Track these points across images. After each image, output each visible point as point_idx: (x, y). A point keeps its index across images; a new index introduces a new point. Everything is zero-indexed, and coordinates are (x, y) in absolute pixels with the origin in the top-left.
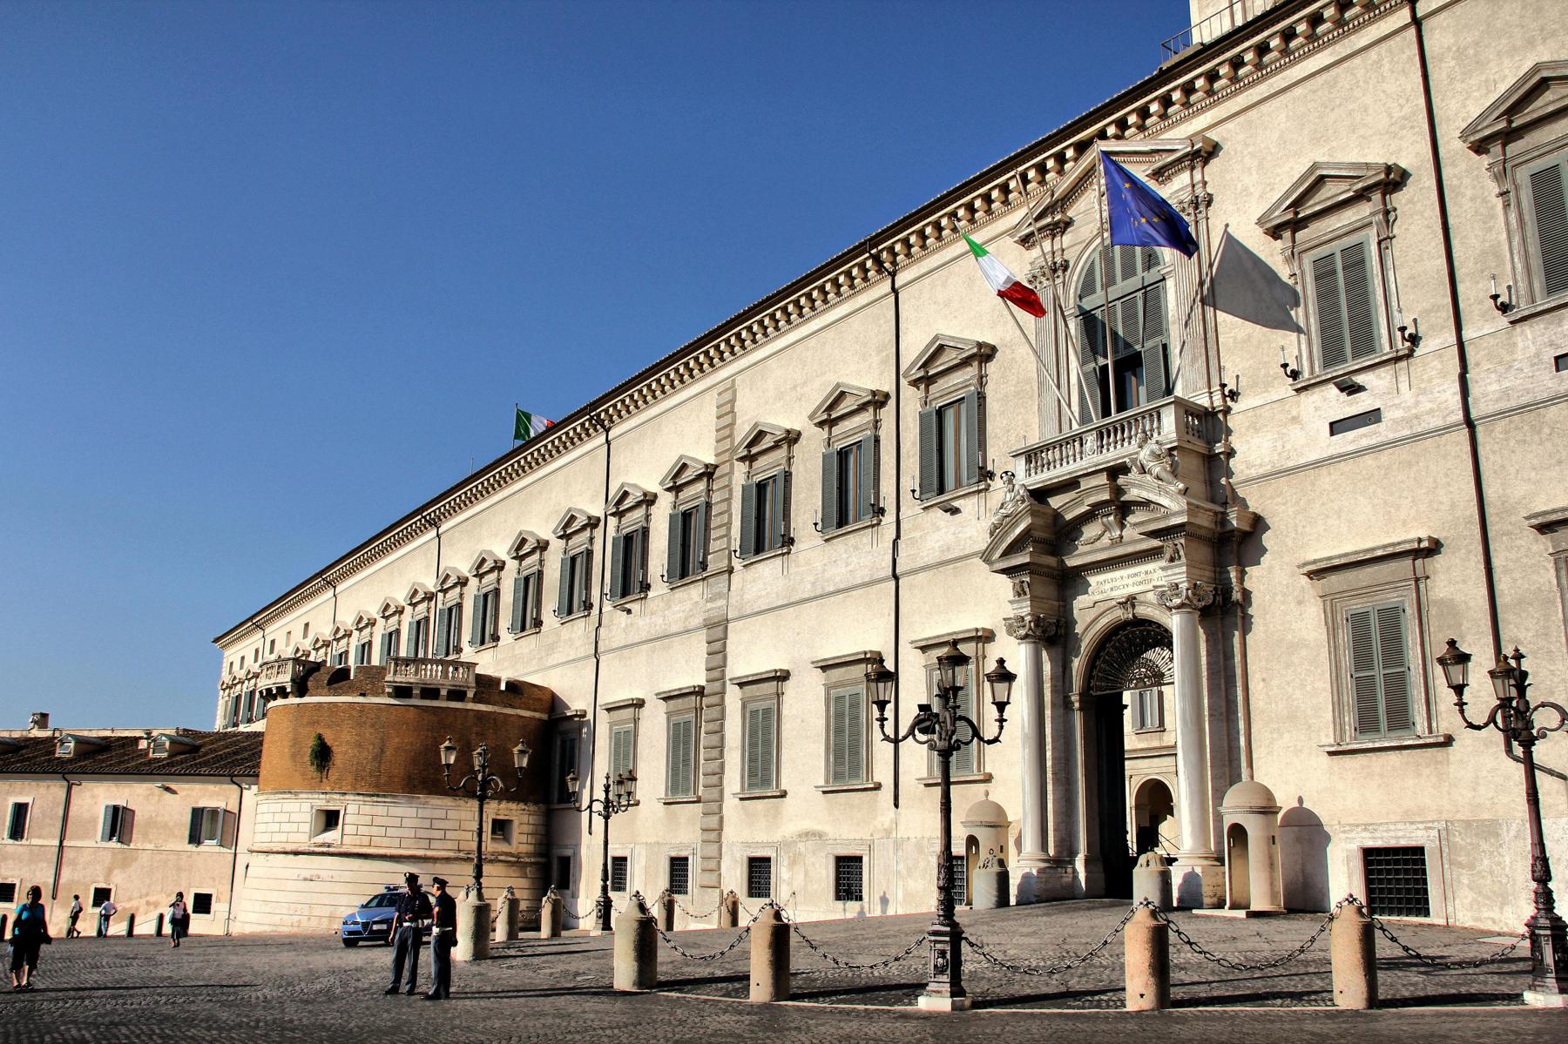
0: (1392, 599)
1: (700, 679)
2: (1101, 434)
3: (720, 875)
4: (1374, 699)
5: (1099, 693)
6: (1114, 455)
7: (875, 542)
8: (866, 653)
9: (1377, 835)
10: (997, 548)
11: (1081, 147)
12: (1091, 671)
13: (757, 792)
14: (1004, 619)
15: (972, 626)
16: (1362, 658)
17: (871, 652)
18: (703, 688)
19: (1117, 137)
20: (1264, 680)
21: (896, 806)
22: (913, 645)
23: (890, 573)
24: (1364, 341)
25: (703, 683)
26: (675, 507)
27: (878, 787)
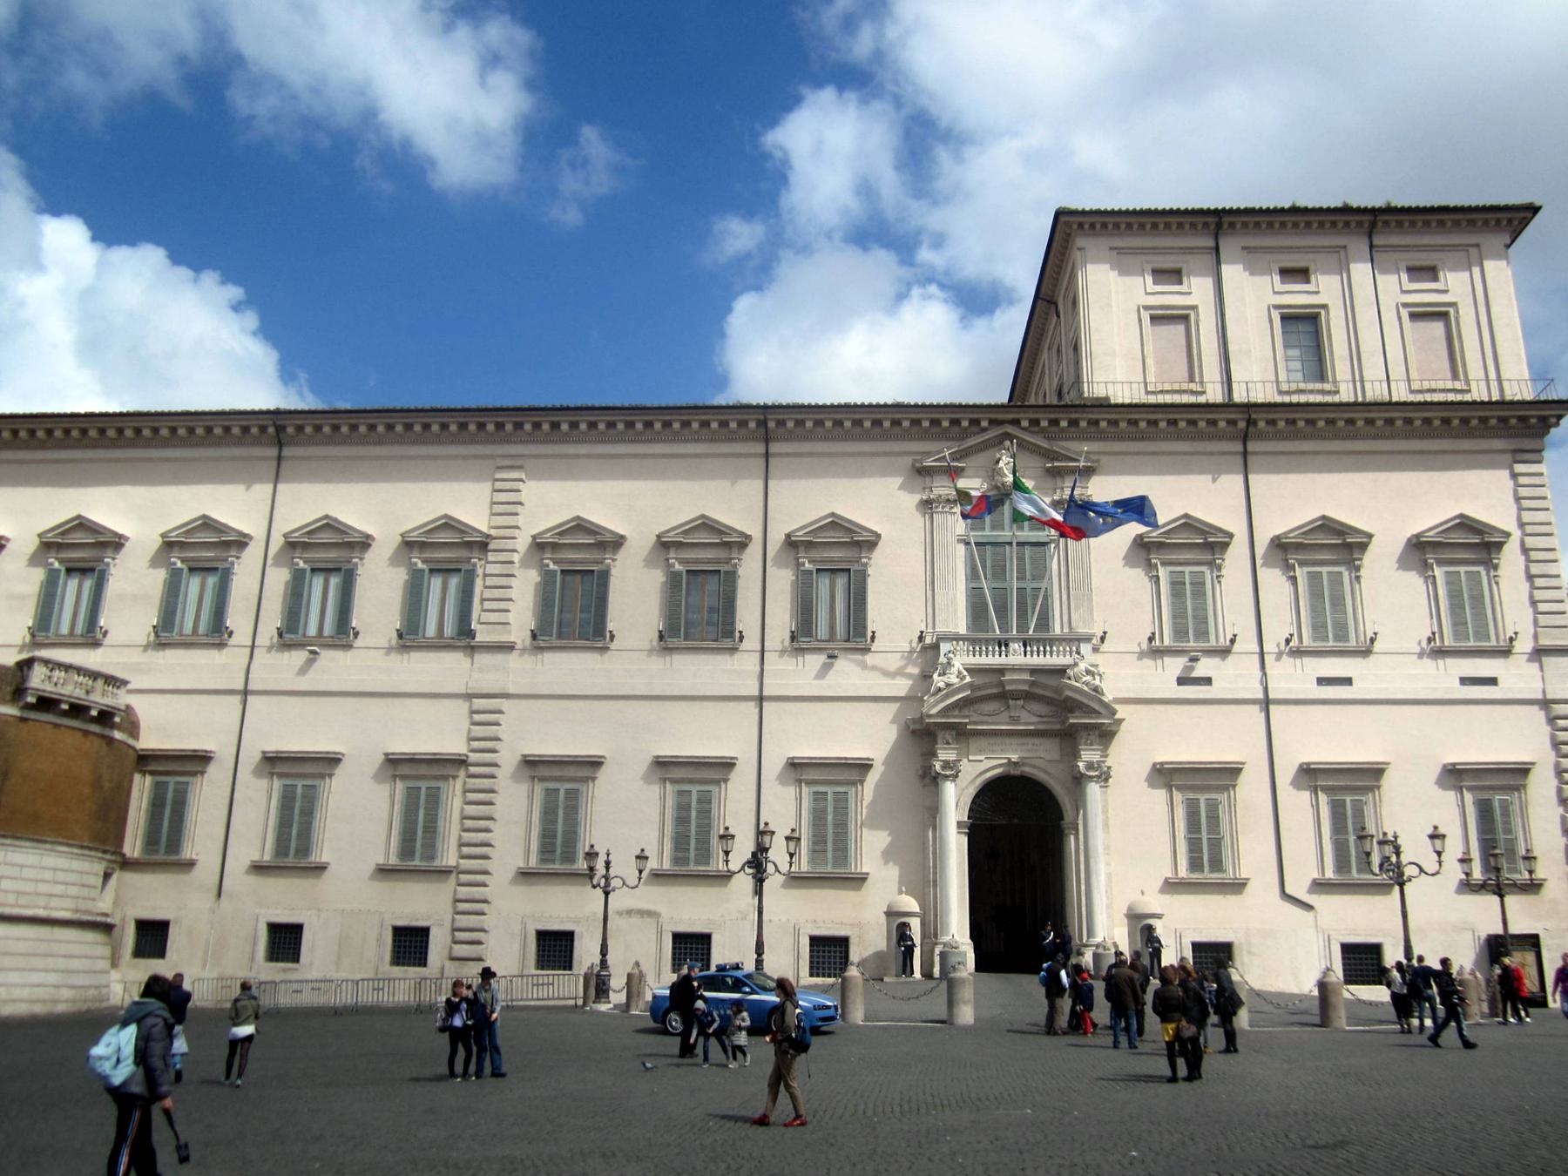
1: (455, 745)
2: (1025, 646)
4: (1201, 851)
11: (993, 422)
13: (557, 867)
19: (1024, 429)
24: (1202, 634)
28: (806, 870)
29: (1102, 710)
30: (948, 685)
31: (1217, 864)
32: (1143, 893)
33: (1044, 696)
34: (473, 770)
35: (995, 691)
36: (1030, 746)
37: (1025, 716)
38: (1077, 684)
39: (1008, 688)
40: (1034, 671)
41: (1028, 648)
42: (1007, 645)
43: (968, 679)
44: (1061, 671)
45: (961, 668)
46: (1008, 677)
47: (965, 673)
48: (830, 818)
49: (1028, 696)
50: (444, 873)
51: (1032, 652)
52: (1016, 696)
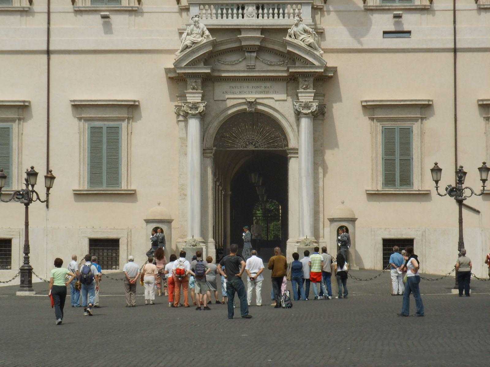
0: (406, 124)
2: (258, 8)
6: (268, 21)
16: (388, 149)
28: (86, 188)
29: (316, 63)
30: (194, 43)
31: (406, 180)
32: (343, 203)
33: (273, 49)
35: (234, 45)
36: (263, 89)
37: (260, 65)
38: (295, 41)
39: (243, 44)
40: (264, 30)
41: (260, 11)
42: (243, 8)
43: (211, 38)
44: (284, 31)
45: (205, 29)
46: (243, 35)
47: (207, 33)
48: (105, 147)
49: (260, 50)
51: (263, 14)
52: (250, 49)
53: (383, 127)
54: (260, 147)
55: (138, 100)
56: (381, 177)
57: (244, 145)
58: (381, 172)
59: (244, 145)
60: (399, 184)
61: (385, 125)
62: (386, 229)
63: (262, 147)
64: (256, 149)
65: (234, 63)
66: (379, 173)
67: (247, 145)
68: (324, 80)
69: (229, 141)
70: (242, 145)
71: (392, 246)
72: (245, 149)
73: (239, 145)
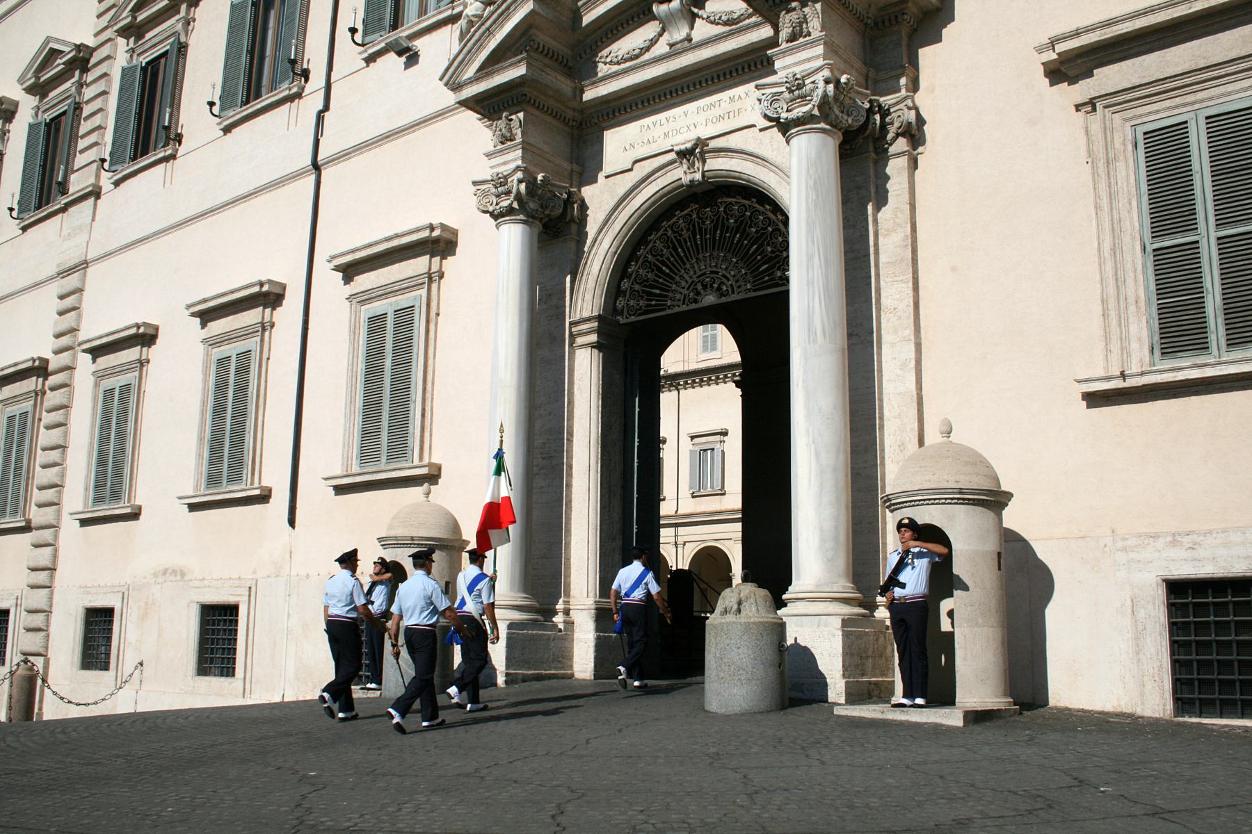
1: (44, 348)
3: (48, 636)
4: (1196, 285)
5: (633, 319)
7: (293, 121)
8: (261, 284)
9: (1201, 553)
10: (471, 61)
12: (627, 265)
14: (475, 183)
15: (424, 222)
17: (270, 282)
18: (47, 361)
20: (954, 269)
21: (292, 522)
22: (332, 265)
23: (308, 161)
25: (48, 354)
26: (37, 114)
27: (264, 497)
34: (52, 380)
37: (702, 30)
48: (388, 363)
50: (27, 528)
53: (1138, 128)
54: (733, 293)
55: (455, 227)
56: (1144, 321)
57: (691, 294)
58: (1142, 304)
59: (691, 294)
60: (1223, 342)
61: (1145, 120)
62: (1178, 538)
63: (740, 290)
64: (724, 300)
65: (637, 51)
66: (1132, 308)
67: (698, 294)
68: (900, 19)
69: (653, 291)
70: (685, 296)
71: (1211, 609)
72: (694, 306)
73: (678, 296)
